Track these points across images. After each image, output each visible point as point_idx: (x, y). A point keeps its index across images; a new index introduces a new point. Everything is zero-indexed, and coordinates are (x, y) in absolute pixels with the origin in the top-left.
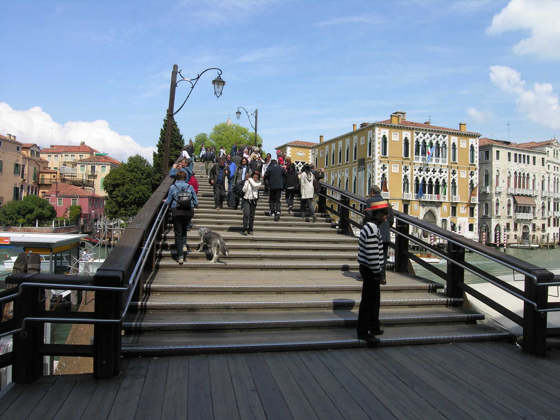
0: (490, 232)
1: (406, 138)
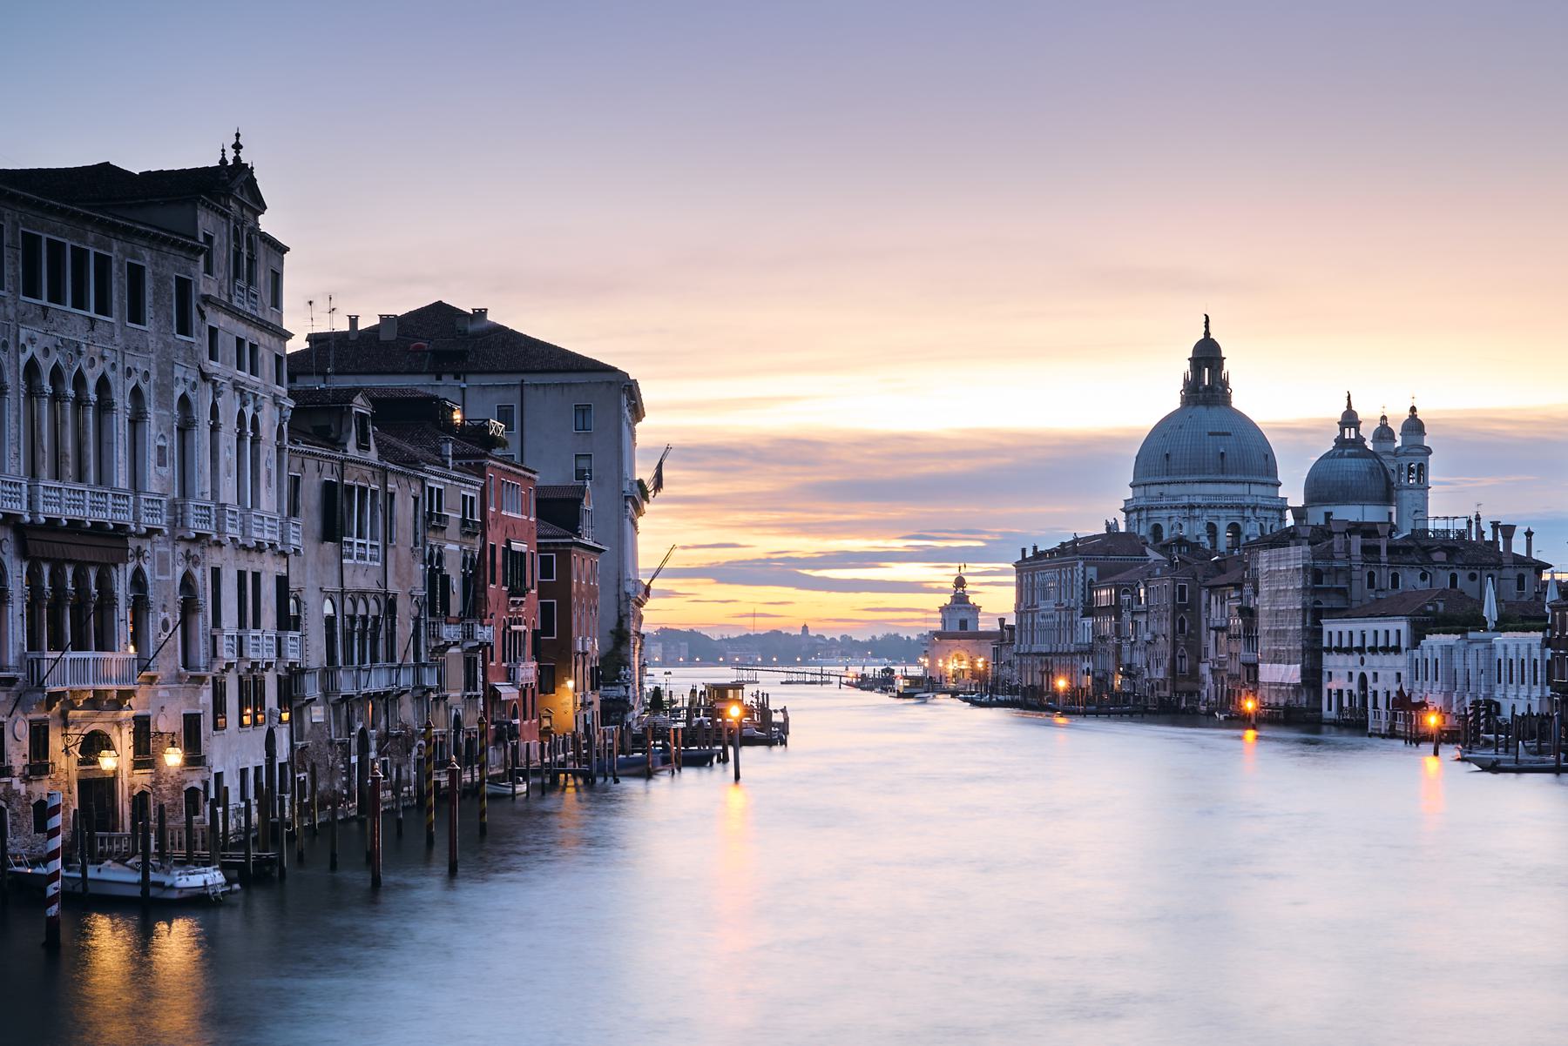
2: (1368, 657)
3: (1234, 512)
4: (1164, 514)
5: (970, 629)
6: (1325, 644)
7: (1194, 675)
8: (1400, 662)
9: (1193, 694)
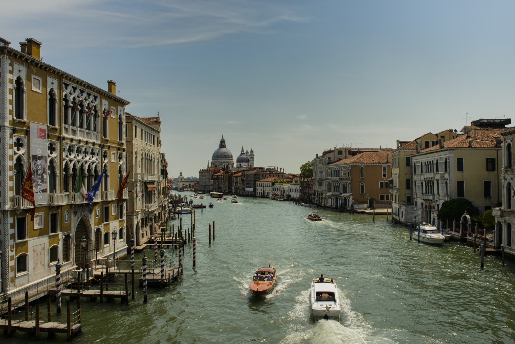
0: (132, 233)
1: (52, 90)
2: (265, 187)
3: (227, 164)
4: (217, 164)
5: (183, 180)
6: (257, 185)
7: (231, 189)
8: (271, 188)
9: (232, 192)
